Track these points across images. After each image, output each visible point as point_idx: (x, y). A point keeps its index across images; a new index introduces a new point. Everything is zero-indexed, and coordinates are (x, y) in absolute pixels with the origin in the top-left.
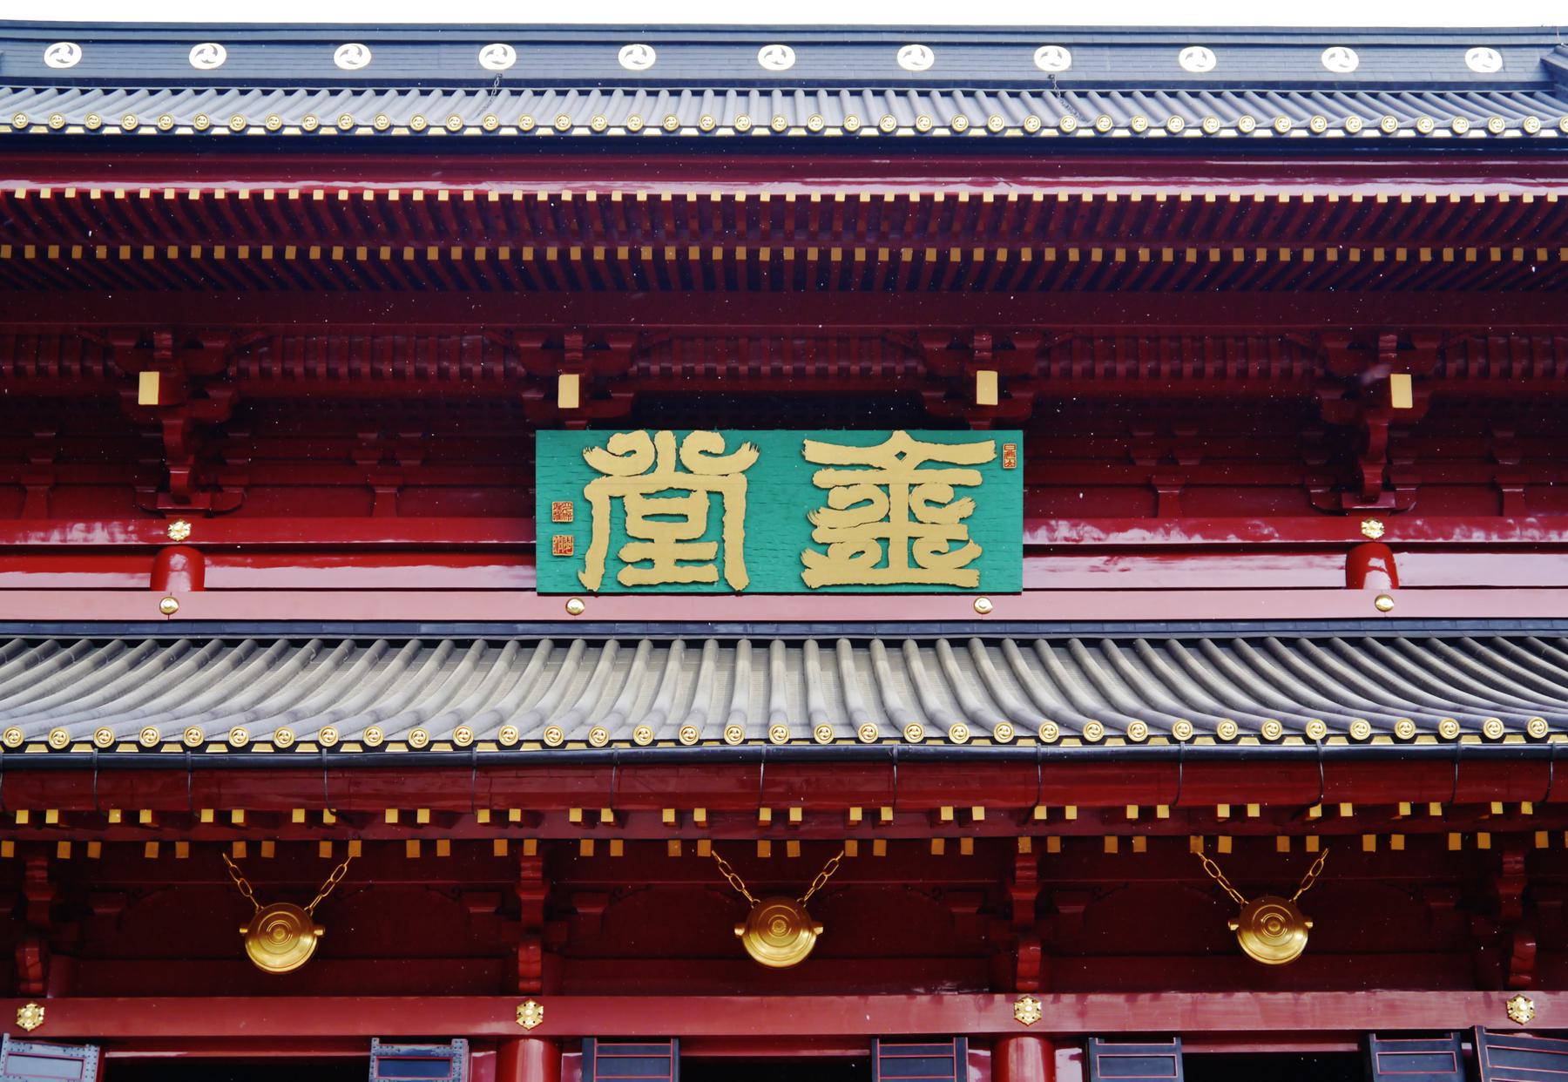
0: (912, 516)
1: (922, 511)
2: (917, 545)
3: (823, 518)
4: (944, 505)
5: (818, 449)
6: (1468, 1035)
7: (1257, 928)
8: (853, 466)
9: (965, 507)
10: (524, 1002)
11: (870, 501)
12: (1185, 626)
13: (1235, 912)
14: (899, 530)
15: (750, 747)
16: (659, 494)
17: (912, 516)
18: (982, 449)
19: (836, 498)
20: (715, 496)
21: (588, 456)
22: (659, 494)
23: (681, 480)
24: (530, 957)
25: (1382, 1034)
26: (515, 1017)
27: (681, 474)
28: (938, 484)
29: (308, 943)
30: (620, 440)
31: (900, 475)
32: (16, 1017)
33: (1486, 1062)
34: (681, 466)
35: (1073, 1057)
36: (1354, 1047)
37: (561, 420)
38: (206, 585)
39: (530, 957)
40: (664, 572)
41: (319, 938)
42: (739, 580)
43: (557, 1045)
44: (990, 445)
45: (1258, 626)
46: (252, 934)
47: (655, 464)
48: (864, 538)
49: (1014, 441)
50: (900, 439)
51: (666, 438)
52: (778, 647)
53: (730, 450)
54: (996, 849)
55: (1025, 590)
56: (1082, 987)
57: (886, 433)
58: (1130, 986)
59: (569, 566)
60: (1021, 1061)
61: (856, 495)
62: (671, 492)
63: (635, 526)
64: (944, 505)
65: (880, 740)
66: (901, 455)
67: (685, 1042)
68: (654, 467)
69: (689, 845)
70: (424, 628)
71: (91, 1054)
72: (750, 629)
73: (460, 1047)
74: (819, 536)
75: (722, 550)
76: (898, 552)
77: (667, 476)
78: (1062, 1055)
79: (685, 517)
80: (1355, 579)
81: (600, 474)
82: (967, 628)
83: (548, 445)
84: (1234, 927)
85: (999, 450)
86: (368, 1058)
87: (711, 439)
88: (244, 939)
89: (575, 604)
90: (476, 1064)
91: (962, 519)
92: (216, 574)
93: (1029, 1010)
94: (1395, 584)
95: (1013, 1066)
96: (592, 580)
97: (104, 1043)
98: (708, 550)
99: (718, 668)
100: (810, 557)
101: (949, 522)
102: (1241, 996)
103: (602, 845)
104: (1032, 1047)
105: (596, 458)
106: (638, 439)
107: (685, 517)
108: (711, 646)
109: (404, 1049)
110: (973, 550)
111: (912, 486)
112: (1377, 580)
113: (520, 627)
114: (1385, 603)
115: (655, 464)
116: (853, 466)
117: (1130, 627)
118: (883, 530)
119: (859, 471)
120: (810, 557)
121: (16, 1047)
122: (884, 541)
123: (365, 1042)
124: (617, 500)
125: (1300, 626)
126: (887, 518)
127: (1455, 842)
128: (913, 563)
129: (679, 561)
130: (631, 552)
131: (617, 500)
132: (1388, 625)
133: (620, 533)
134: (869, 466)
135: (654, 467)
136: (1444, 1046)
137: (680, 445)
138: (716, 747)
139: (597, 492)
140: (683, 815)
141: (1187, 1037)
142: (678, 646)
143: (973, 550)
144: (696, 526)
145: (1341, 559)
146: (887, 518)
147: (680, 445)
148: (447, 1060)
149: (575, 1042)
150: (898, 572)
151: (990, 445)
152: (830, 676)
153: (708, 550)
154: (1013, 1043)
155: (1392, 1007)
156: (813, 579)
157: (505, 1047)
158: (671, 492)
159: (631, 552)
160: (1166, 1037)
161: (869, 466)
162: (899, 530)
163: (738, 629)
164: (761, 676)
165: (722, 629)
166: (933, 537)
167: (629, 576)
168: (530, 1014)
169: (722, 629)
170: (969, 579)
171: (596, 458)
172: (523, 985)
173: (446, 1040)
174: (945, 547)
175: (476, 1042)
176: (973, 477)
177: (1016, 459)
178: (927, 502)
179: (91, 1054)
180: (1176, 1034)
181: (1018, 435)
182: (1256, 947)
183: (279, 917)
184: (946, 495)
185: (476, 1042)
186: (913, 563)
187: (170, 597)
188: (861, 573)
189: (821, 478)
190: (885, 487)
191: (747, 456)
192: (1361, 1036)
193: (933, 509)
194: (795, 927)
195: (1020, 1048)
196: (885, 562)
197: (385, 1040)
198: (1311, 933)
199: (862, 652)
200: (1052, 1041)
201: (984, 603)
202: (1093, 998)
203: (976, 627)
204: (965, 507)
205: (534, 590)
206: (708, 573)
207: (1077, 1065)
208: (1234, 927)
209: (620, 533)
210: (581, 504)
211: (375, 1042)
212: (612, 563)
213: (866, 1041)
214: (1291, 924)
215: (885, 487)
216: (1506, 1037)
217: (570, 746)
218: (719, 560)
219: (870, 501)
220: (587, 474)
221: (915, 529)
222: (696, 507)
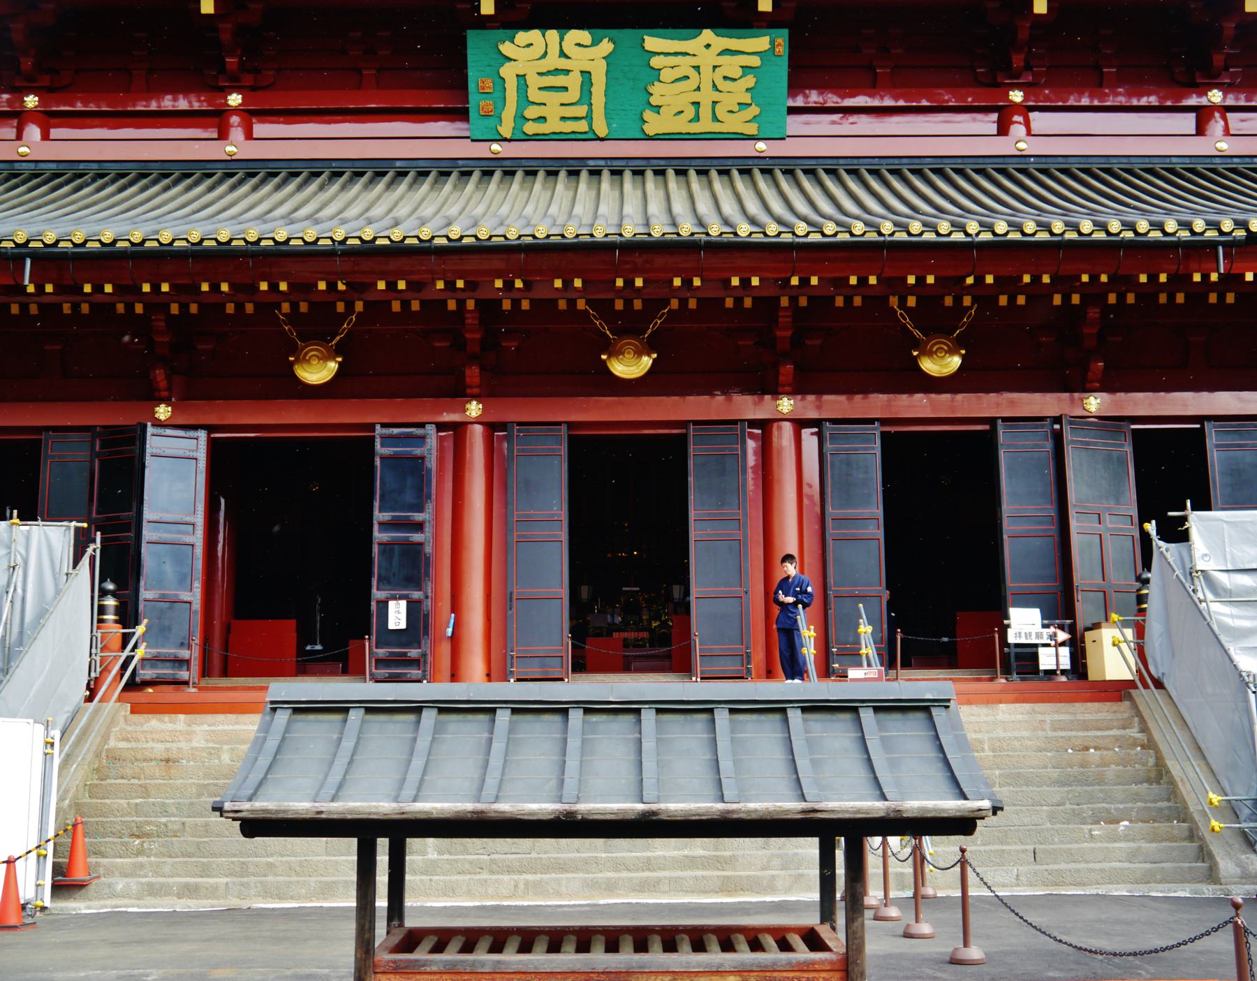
0: (714, 86)
1: (721, 84)
2: (718, 107)
3: (656, 89)
4: (735, 80)
5: (652, 42)
6: (1058, 420)
7: (930, 354)
8: (676, 54)
9: (750, 81)
10: (469, 402)
11: (687, 77)
12: (891, 161)
13: (916, 344)
14: (706, 96)
15: (610, 238)
16: (549, 73)
17: (714, 86)
18: (761, 42)
19: (665, 75)
20: (586, 74)
21: (501, 47)
22: (549, 73)
23: (563, 64)
24: (473, 374)
25: (1005, 419)
26: (464, 410)
27: (563, 59)
28: (732, 66)
29: (333, 366)
30: (522, 37)
31: (707, 59)
32: (154, 413)
33: (1068, 435)
34: (563, 54)
35: (812, 434)
36: (987, 427)
37: (485, 23)
38: (255, 136)
39: (473, 374)
41: (340, 363)
42: (602, 132)
43: (491, 427)
44: (767, 39)
45: (939, 160)
46: (297, 361)
47: (546, 53)
48: (684, 102)
49: (782, 36)
50: (707, 35)
51: (553, 34)
52: (628, 175)
53: (595, 42)
54: (766, 304)
55: (788, 136)
56: (820, 391)
57: (698, 31)
58: (849, 389)
59: (491, 122)
60: (780, 437)
61: (678, 73)
62: (557, 72)
63: (534, 95)
64: (735, 80)
65: (692, 234)
66: (708, 46)
67: (571, 425)
68: (545, 54)
69: (572, 303)
70: (398, 164)
71: (202, 435)
72: (609, 163)
73: (431, 429)
74: (654, 101)
75: (590, 111)
76: (705, 111)
77: (554, 61)
78: (806, 433)
79: (566, 89)
80: (1003, 130)
81: (509, 59)
82: (750, 162)
83: (476, 42)
84: (915, 353)
85: (772, 42)
86: (373, 438)
87: (583, 36)
88: (292, 364)
89: (496, 147)
90: (441, 439)
91: (748, 90)
92: (260, 129)
93: (786, 405)
94: (1029, 133)
95: (775, 440)
96: (506, 131)
97: (210, 429)
98: (581, 111)
99: (589, 188)
100: (648, 115)
101: (739, 91)
102: (918, 396)
103: (516, 303)
104: (787, 428)
105: (506, 48)
106: (534, 35)
107: (566, 89)
108: (584, 175)
109: (396, 431)
110: (754, 110)
111: (715, 67)
112: (1018, 130)
113: (460, 162)
114: (1022, 145)
115: (546, 53)
116: (676, 54)
117: (855, 161)
118: (696, 97)
119: (680, 57)
120: (648, 115)
121: (156, 431)
122: (696, 104)
123: (371, 427)
124: (521, 77)
125: (966, 160)
126: (698, 89)
127: (1003, 300)
128: (715, 119)
129: (563, 118)
130: (531, 112)
132: (1023, 160)
134: (687, 54)
135: (545, 54)
136: (1043, 426)
137: (562, 39)
138: (588, 239)
139: (508, 71)
140: (568, 283)
141: (883, 421)
142: (563, 174)
143: (754, 110)
145: (995, 116)
146: (698, 89)
147: (562, 39)
148: (423, 438)
149: (503, 426)
150: (706, 125)
151: (767, 39)
152: (661, 193)
153: (581, 111)
154: (775, 425)
155: (1012, 403)
156: (650, 130)
157: (459, 430)
158: (557, 72)
159: (531, 112)
160: (870, 421)
161: (687, 54)
162: (706, 96)
163: (602, 163)
164: (617, 193)
165: (591, 163)
166: (729, 102)
167: (530, 128)
168: (474, 409)
169: (591, 163)
170: (751, 129)
171: (506, 48)
172: (469, 391)
173: (422, 425)
174: (736, 108)
175: (441, 427)
176: (755, 61)
177: (783, 49)
178: (725, 78)
179: (202, 435)
180: (877, 419)
181: (785, 32)
182: (930, 366)
183: (313, 351)
184: (737, 73)
185: (441, 427)
186: (715, 119)
187: (232, 144)
188: (681, 126)
189: (656, 62)
190: (697, 68)
191: (606, 47)
192: (992, 421)
193: (728, 82)
194: (639, 353)
195: (780, 428)
196: (697, 118)
197: (384, 425)
198: (964, 357)
199: (682, 178)
200: (800, 424)
201: (761, 146)
202: (826, 397)
203: (756, 162)
204: (750, 81)
205: (468, 138)
206: (582, 126)
207: (815, 438)
208: (915, 353)
210: (498, 80)
211: (378, 427)
212: (518, 119)
213: (684, 424)
214: (952, 352)
215: (697, 68)
216: (1081, 421)
217: (494, 239)
218: (589, 117)
219: (687, 77)
220: (502, 60)
221: (716, 96)
222: (574, 81)
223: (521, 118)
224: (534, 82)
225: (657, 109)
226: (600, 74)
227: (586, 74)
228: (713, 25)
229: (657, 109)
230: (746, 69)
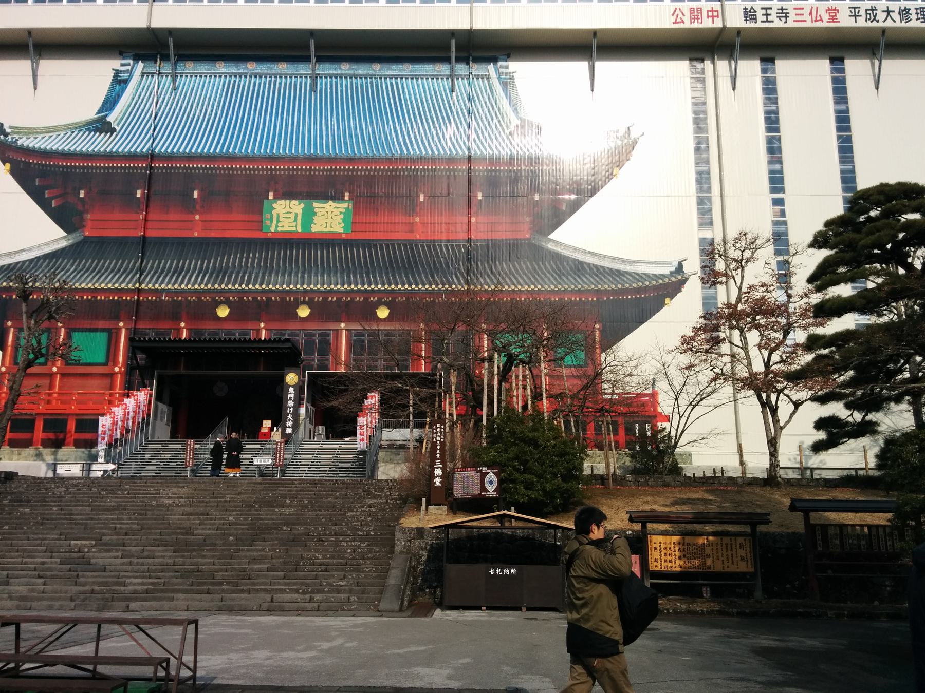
1: (334, 217)
5: (315, 204)
18: (346, 205)
20: (296, 214)
23: (290, 210)
28: (337, 211)
31: (330, 209)
40: (286, 229)
42: (300, 230)
50: (331, 202)
51: (288, 201)
62: (288, 213)
63: (281, 219)
76: (329, 225)
98: (294, 224)
105: (274, 205)
106: (282, 202)
120: (313, 225)
124: (278, 215)
130: (280, 224)
131: (278, 215)
133: (278, 221)
139: (274, 212)
143: (343, 225)
144: (292, 219)
156: (313, 230)
158: (288, 213)
167: (280, 229)
171: (274, 205)
176: (344, 211)
189: (316, 210)
191: (302, 206)
204: (342, 216)
206: (294, 229)
209: (278, 221)
218: (296, 226)
221: (331, 220)
222: (293, 216)
223: (277, 226)
224: (281, 216)
225: (315, 224)
226: (300, 212)
227: (296, 214)
228: (332, 199)
229: (315, 224)
230: (341, 213)
